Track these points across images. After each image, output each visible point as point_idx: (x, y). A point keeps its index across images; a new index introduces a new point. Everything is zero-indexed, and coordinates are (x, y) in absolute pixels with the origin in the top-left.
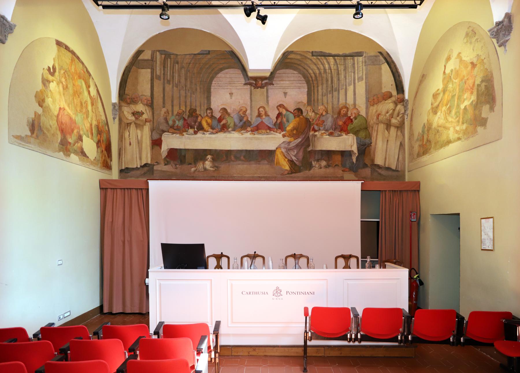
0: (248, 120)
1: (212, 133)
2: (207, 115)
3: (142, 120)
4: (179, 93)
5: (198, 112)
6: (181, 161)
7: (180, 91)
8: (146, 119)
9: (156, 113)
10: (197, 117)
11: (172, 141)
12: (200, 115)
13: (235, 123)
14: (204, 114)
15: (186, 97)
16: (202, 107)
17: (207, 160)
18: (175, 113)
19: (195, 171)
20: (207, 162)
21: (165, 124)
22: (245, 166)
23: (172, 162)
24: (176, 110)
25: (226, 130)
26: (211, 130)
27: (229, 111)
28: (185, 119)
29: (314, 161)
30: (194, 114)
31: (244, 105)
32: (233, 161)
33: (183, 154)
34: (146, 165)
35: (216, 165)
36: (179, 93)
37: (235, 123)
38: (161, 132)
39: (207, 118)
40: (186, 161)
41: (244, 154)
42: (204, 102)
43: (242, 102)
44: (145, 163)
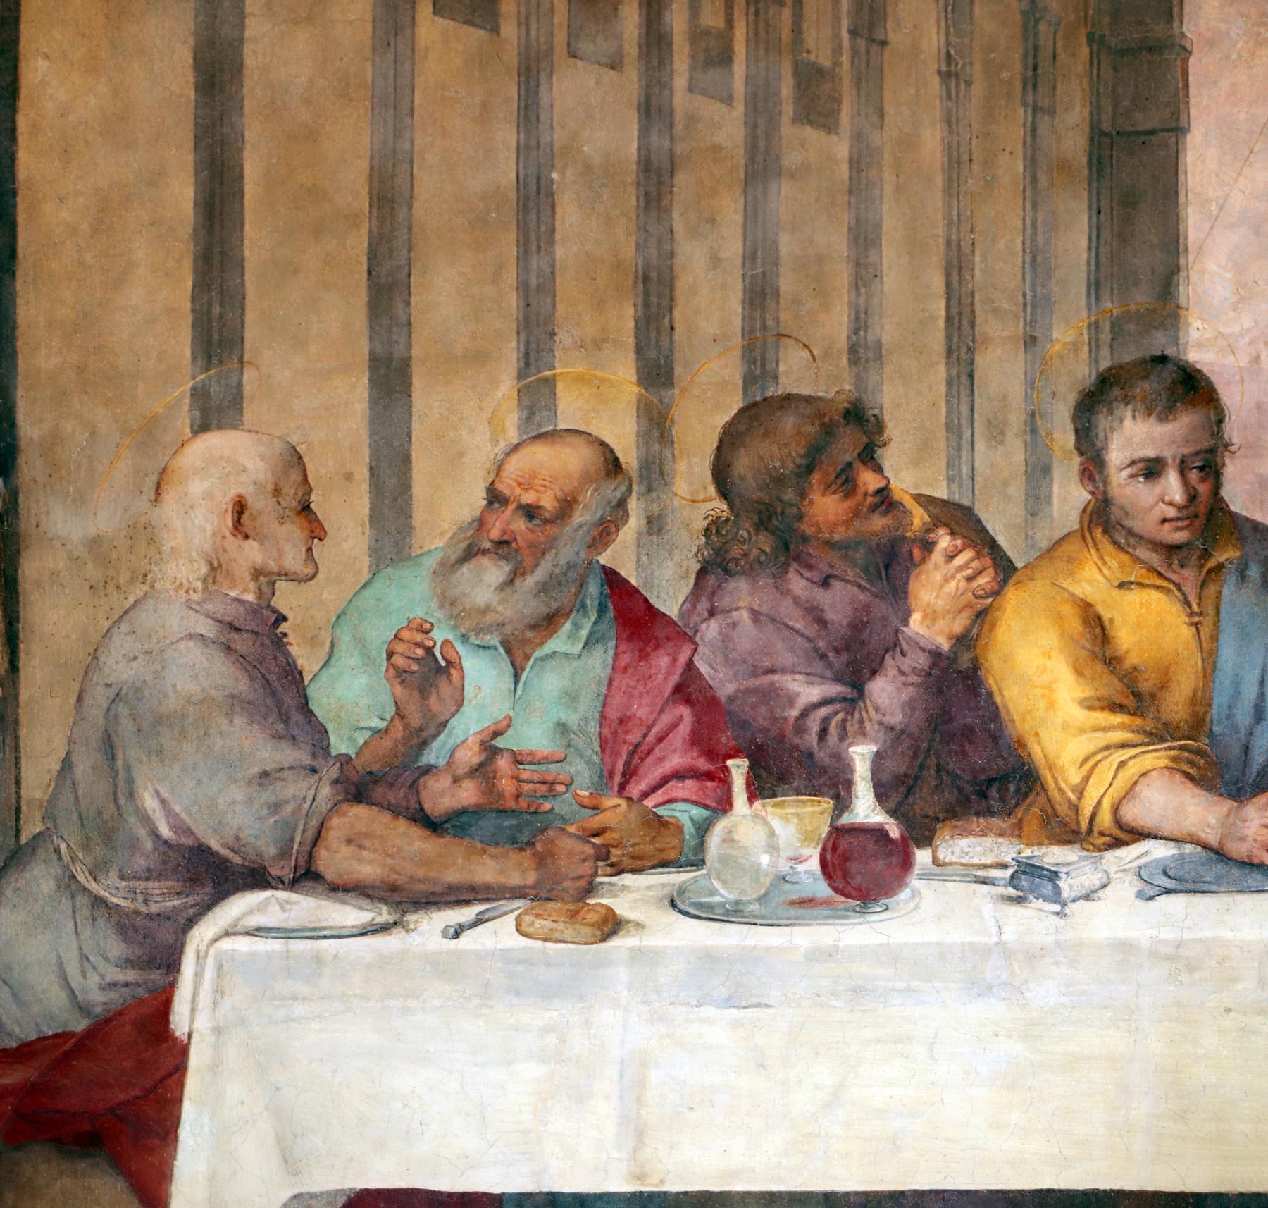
4: (529, 112)
5: (909, 471)
7: (532, 71)
10: (891, 565)
12: (960, 519)
15: (655, 182)
16: (1002, 370)
18: (447, 502)
24: (468, 441)
26: (1199, 812)
30: (826, 507)
36: (529, 112)
38: (164, 899)
39: (1093, 578)
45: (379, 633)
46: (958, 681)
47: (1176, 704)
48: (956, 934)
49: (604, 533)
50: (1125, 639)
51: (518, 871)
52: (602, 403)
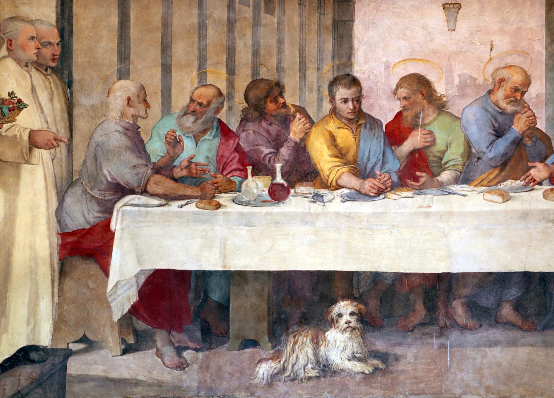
0: (532, 128)
1: (359, 195)
2: (334, 112)
3: (14, 140)
6: (206, 331)
8: (32, 134)
9: (84, 101)
10: (286, 121)
11: (157, 238)
13: (468, 145)
14: (316, 104)
17: (332, 323)
19: (274, 378)
20: (332, 335)
21: (132, 159)
22: (523, 352)
23: (160, 337)
24: (185, 86)
25: (424, 177)
27: (440, 88)
28: (225, 131)
31: (517, 60)
32: (464, 328)
33: (216, 296)
34: (24, 356)
35: (380, 345)
37: (468, 145)
39: (332, 126)
40: (233, 328)
41: (513, 293)
42: (320, 50)
43: (503, 43)
44: (23, 343)
45: (163, 132)
46: (301, 150)
47: (350, 157)
48: (299, 210)
49: (218, 110)
50: (339, 141)
51: (196, 192)
52: (218, 79)
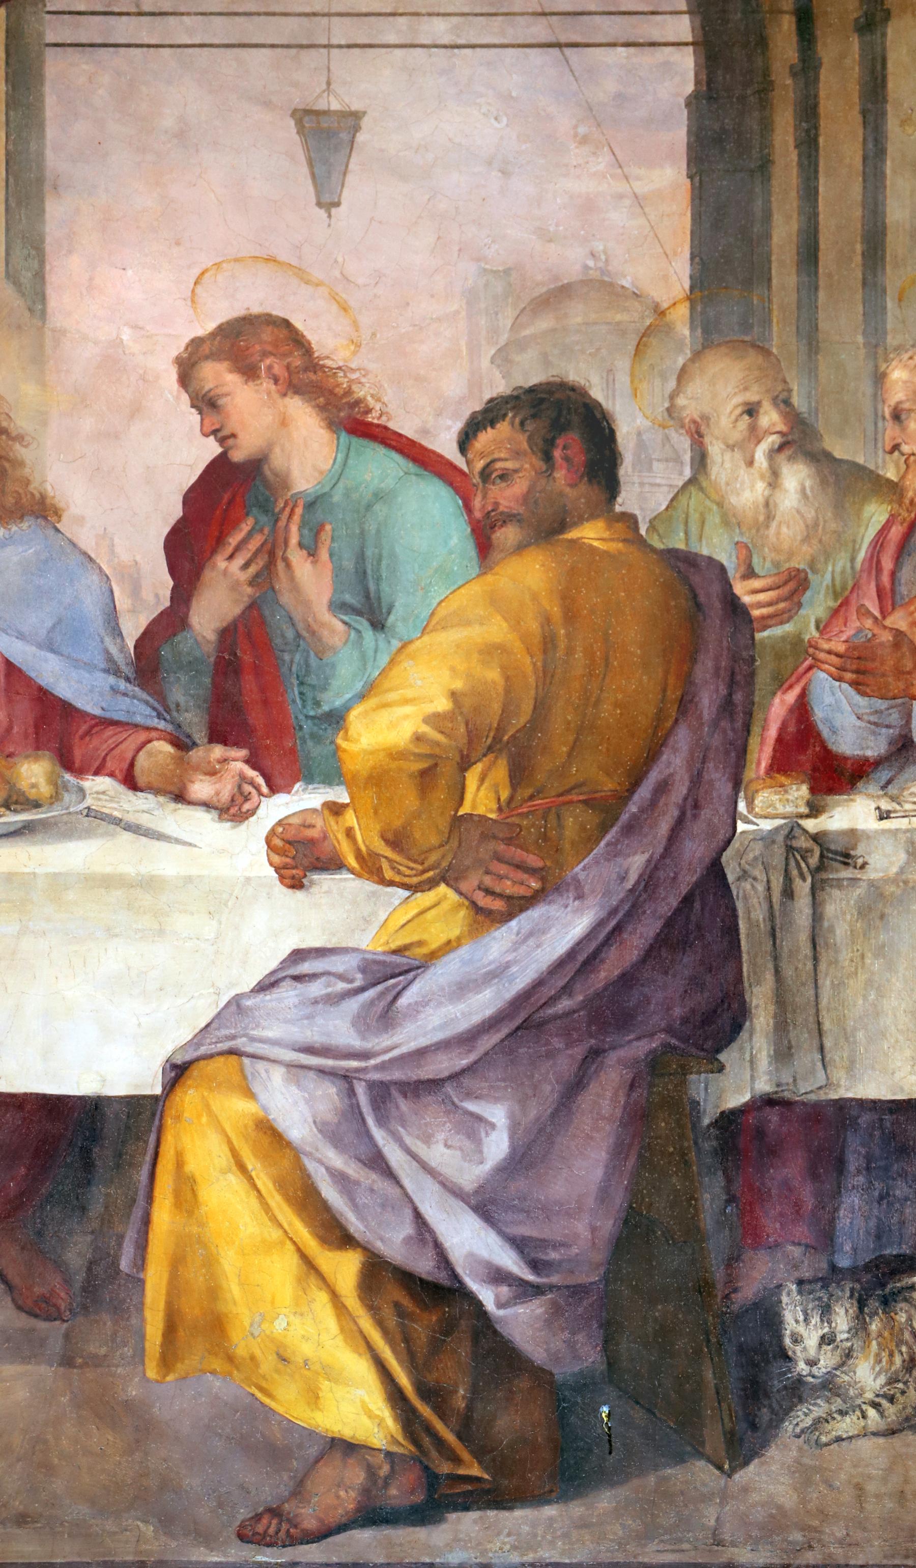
29: (822, 1285)
